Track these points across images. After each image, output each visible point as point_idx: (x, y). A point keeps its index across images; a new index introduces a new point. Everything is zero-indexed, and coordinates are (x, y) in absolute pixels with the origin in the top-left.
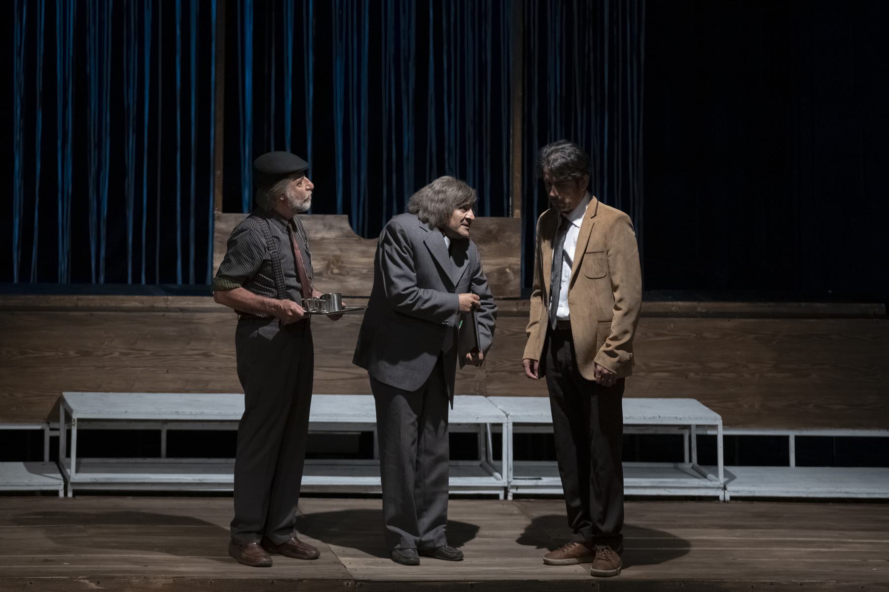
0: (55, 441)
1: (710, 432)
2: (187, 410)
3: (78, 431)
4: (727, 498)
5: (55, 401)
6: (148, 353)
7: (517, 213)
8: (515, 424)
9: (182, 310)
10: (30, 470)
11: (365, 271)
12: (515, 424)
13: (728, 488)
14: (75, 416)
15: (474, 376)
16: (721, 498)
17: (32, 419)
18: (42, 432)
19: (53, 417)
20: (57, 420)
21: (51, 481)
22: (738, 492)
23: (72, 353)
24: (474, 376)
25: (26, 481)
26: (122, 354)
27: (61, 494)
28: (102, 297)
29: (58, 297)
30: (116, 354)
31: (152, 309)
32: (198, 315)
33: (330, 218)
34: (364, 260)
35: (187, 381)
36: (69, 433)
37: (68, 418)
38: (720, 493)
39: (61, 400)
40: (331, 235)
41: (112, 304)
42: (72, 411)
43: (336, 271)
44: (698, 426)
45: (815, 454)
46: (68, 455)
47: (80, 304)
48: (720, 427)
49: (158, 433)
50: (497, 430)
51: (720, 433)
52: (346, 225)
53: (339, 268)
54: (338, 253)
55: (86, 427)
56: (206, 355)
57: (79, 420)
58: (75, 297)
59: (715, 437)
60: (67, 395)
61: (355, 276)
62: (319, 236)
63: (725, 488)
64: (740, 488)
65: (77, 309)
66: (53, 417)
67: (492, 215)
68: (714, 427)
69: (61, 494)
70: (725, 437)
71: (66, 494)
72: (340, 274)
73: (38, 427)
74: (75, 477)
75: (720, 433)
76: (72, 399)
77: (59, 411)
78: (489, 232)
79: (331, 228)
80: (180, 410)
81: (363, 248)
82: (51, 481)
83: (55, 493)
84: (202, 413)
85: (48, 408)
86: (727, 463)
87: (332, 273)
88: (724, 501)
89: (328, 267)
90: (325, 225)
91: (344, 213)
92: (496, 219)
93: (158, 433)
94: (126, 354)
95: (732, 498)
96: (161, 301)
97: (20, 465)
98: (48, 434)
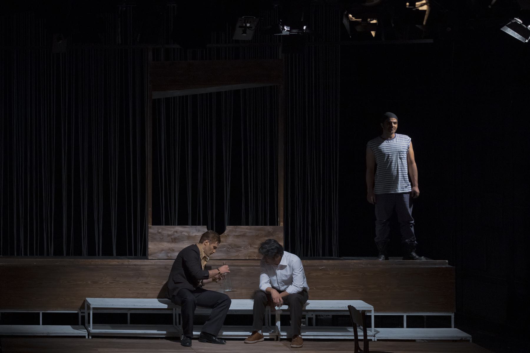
0: (83, 317)
1: (368, 314)
2: (139, 304)
3: (93, 314)
4: (376, 340)
5: (83, 301)
7: (282, 224)
9: (135, 265)
10: (74, 328)
13: (376, 335)
14: (91, 307)
16: (373, 340)
18: (77, 314)
19: (83, 307)
20: (84, 309)
21: (83, 332)
23: (89, 282)
25: (72, 332)
26: (110, 283)
27: (87, 337)
30: (108, 283)
32: (142, 267)
33: (199, 227)
35: (138, 293)
36: (89, 314)
38: (373, 338)
39: (85, 301)
42: (90, 304)
45: (413, 322)
46: (89, 323)
48: (373, 312)
49: (127, 314)
50: (273, 313)
51: (373, 314)
55: (96, 312)
56: (146, 283)
57: (94, 308)
60: (87, 299)
62: (194, 234)
63: (374, 336)
64: (381, 336)
67: (270, 225)
68: (370, 311)
69: (87, 337)
70: (375, 316)
71: (89, 337)
73: (76, 312)
74: (93, 331)
75: (373, 314)
76: (90, 300)
77: (85, 306)
78: (269, 232)
79: (199, 231)
80: (136, 304)
82: (83, 332)
83: (84, 337)
84: (145, 306)
85: (80, 304)
91: (203, 225)
92: (272, 227)
93: (127, 314)
94: (112, 283)
95: (378, 340)
97: (69, 326)
98: (80, 315)
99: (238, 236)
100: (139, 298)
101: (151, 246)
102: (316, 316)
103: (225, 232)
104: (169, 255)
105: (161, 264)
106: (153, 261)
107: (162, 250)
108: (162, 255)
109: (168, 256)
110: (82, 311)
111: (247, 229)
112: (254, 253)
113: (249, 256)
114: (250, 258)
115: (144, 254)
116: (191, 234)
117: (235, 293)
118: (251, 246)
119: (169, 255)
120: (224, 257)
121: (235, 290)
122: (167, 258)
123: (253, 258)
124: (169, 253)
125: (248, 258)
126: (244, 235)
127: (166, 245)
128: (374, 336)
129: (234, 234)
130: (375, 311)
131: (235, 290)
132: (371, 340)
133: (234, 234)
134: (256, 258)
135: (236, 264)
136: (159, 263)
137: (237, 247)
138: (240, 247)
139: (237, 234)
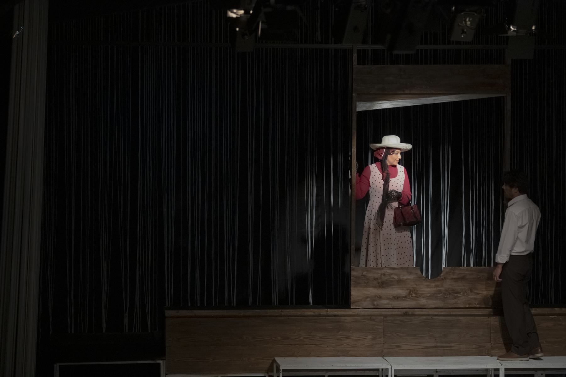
5: (271, 362)
6: (318, 337)
8: (506, 369)
9: (335, 316)
11: (428, 295)
12: (506, 369)
14: (281, 368)
15: (485, 346)
17: (259, 371)
19: (270, 369)
20: (273, 372)
23: (279, 338)
24: (485, 346)
28: (294, 310)
29: (271, 311)
30: (302, 338)
31: (320, 315)
32: (343, 318)
37: (278, 370)
39: (274, 361)
40: (411, 277)
41: (299, 314)
42: (279, 366)
43: (414, 295)
47: (283, 314)
50: (496, 373)
53: (415, 294)
54: (415, 286)
55: (287, 374)
56: (347, 338)
58: (280, 310)
60: (277, 359)
61: (423, 297)
62: (405, 278)
65: (281, 316)
66: (270, 369)
72: (416, 297)
81: (428, 283)
89: (410, 293)
90: (408, 272)
96: (323, 312)
99: (456, 280)
100: (339, 356)
101: (355, 293)
104: (375, 303)
105: (366, 314)
106: (356, 312)
107: (367, 297)
108: (366, 304)
109: (374, 305)
110: (271, 374)
111: (467, 270)
112: (475, 299)
113: (469, 304)
114: (471, 306)
115: (344, 301)
116: (401, 277)
117: (453, 348)
118: (471, 292)
119: (375, 303)
120: (440, 305)
121: (452, 345)
122: (373, 307)
123: (473, 306)
124: (374, 300)
125: (467, 306)
126: (463, 278)
127: (372, 291)
129: (452, 276)
131: (452, 345)
133: (452, 276)
134: (478, 306)
135: (454, 313)
136: (363, 313)
137: (454, 293)
138: (459, 293)
139: (455, 277)
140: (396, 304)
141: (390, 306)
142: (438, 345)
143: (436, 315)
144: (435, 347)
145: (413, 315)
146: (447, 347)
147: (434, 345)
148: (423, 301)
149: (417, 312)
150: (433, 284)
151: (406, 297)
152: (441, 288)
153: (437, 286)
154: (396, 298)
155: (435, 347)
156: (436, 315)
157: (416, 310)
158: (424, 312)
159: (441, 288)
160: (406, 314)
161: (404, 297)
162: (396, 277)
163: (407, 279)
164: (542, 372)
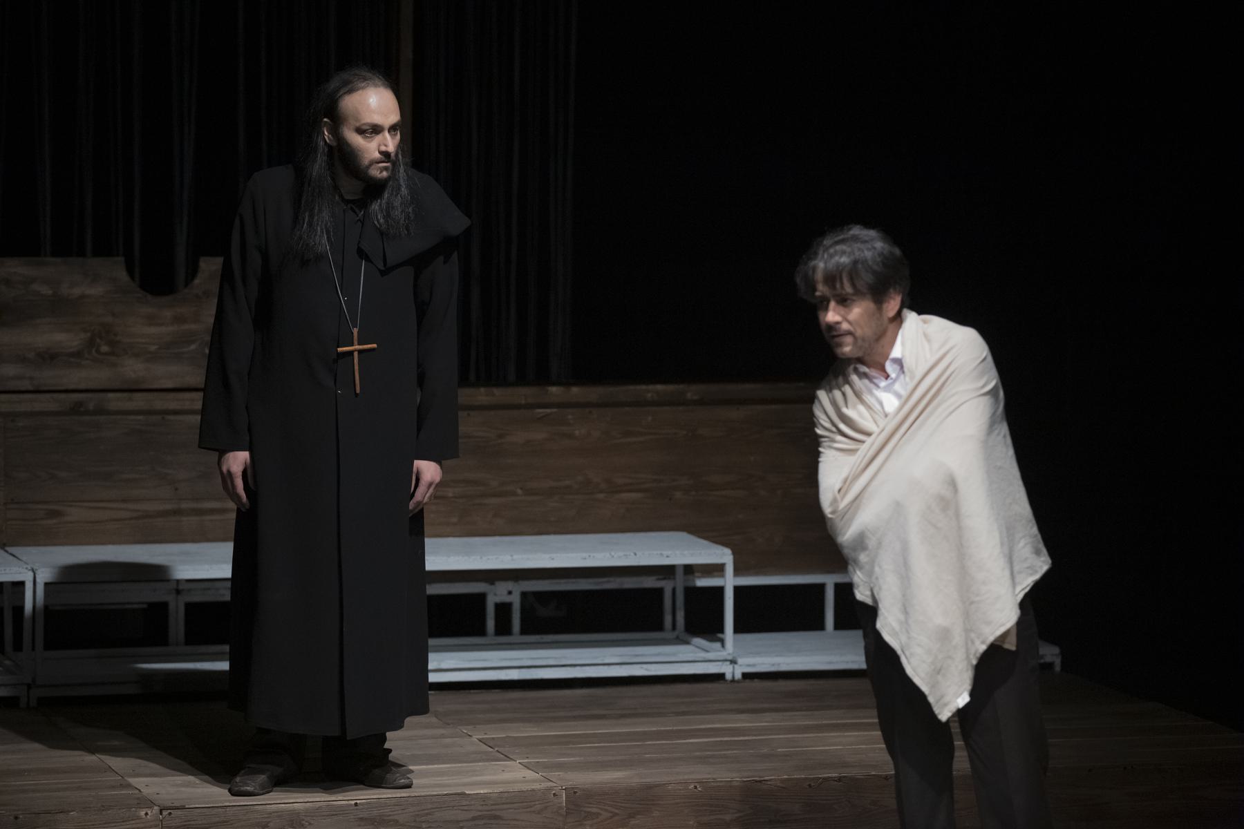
4: (738, 676)
11: (153, 348)
13: (740, 661)
16: (729, 677)
22: (754, 665)
34: (153, 330)
38: (727, 669)
40: (96, 290)
43: (105, 349)
44: (689, 569)
48: (729, 569)
51: (729, 582)
52: (123, 275)
59: (720, 591)
62: (77, 291)
68: (718, 569)
75: (729, 582)
86: (737, 630)
87: (98, 351)
88: (733, 681)
95: (746, 676)
102: (524, 595)
103: (197, 281)
128: (733, 662)
130: (738, 571)
132: (720, 677)
140: (49, 376)
141: (26, 385)
142: (184, 505)
143: (176, 412)
144: (177, 512)
145: (100, 411)
146: (212, 511)
147: (168, 507)
148: (133, 369)
149: (115, 401)
150: (168, 314)
151: (78, 354)
152: (193, 327)
153: (179, 320)
154: (49, 357)
155: (177, 512)
156: (176, 412)
157: (111, 395)
158: (139, 401)
159: (193, 327)
160: (77, 409)
161: (72, 355)
162: (46, 290)
163: (83, 297)
164: (510, 585)
